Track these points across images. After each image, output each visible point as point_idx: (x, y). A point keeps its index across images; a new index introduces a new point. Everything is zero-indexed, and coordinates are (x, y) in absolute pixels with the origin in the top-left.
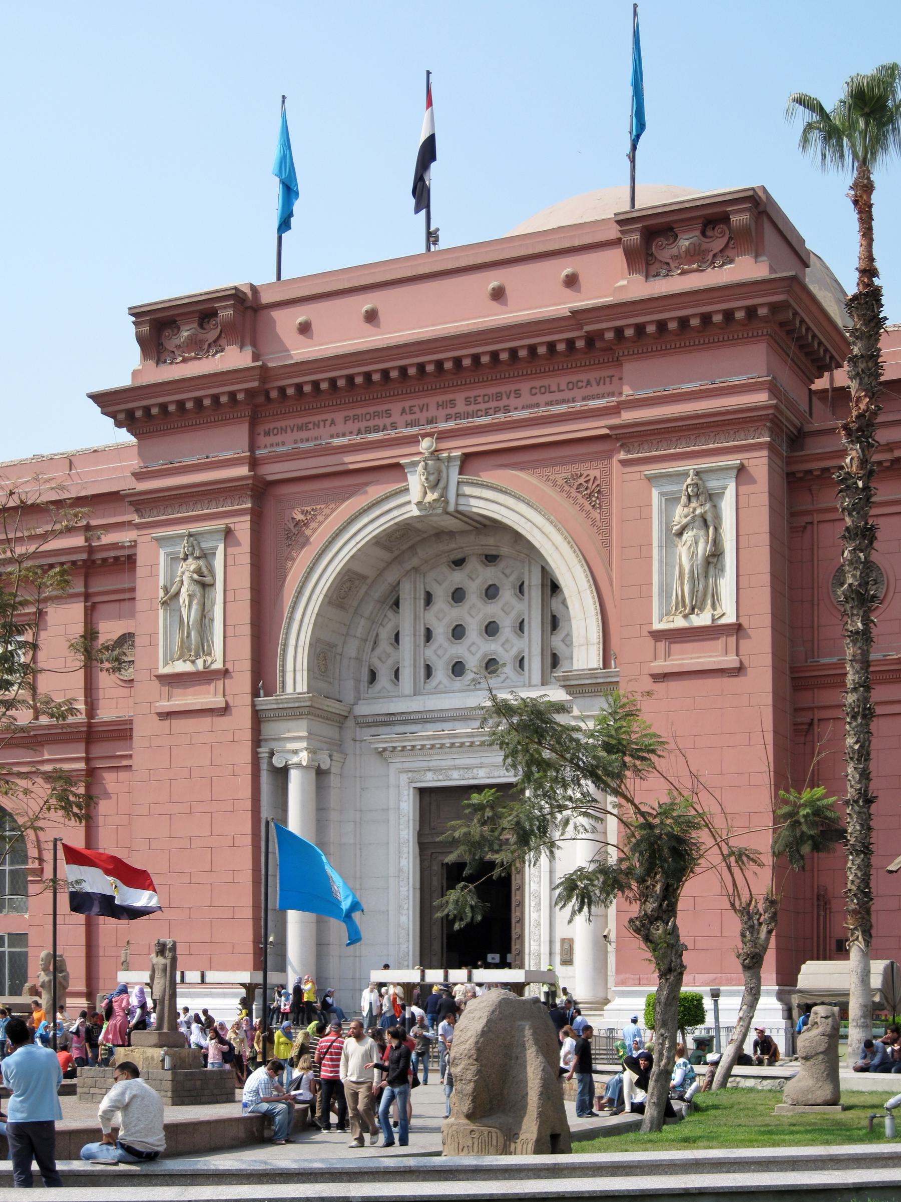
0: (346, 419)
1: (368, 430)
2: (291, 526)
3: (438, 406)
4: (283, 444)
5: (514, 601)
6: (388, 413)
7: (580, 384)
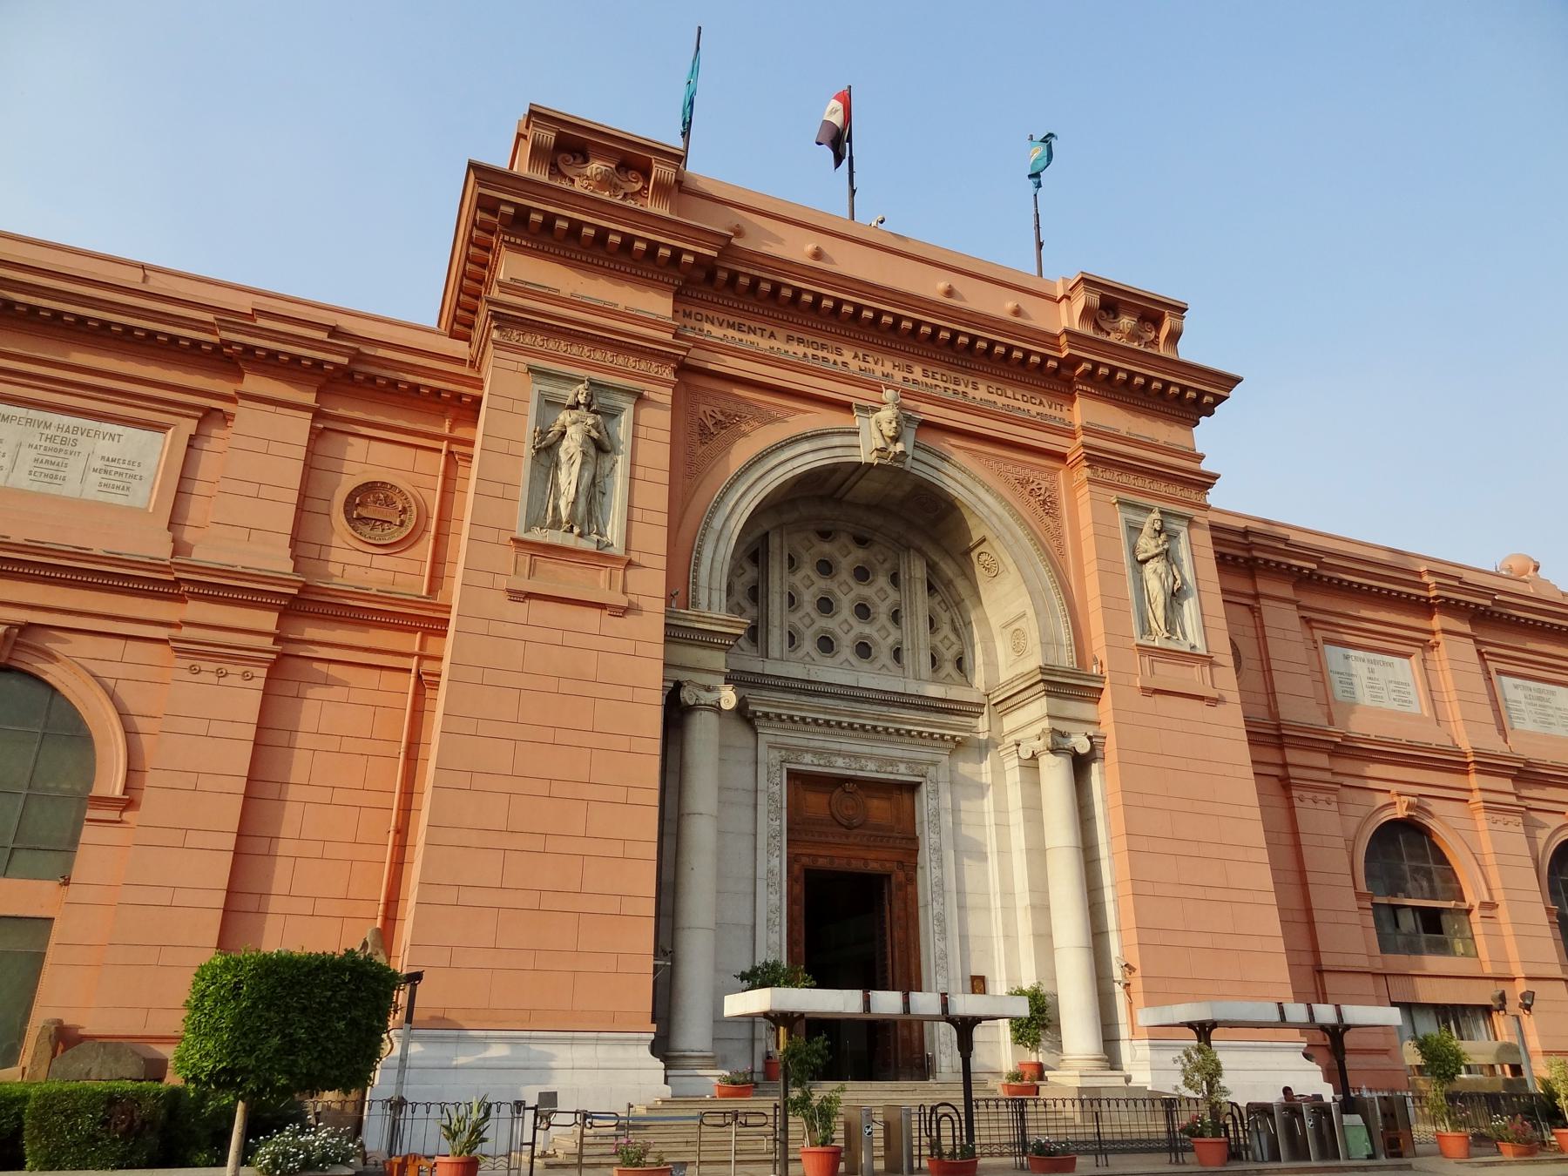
0: (790, 339)
5: (890, 589)
6: (839, 352)
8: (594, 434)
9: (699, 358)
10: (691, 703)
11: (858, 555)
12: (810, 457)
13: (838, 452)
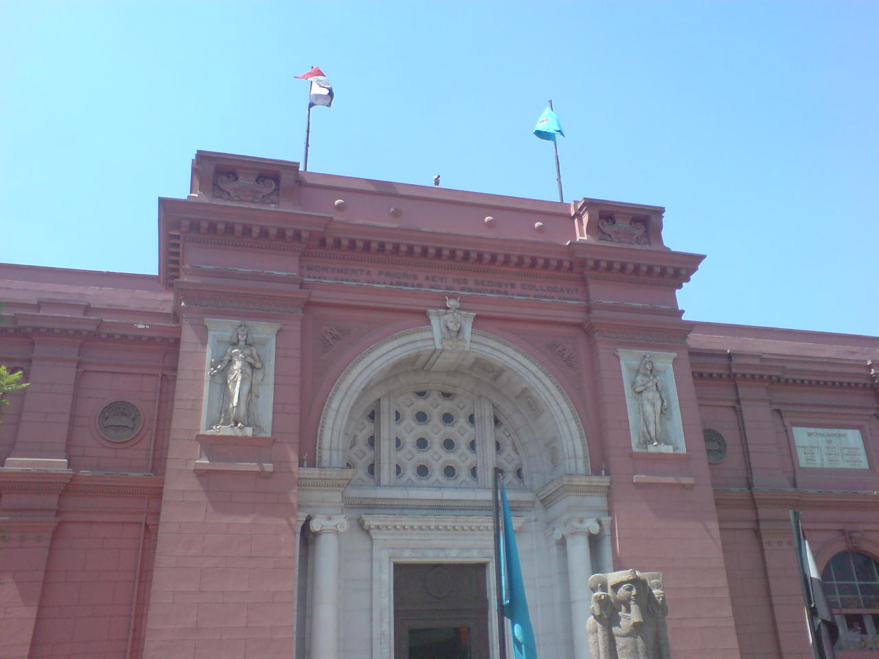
0: (380, 273)
1: (399, 284)
2: (329, 338)
3: (454, 281)
4: (325, 278)
5: (467, 426)
6: (415, 277)
7: (556, 290)
8: (249, 359)
9: (318, 296)
10: (317, 530)
11: (447, 406)
12: (399, 351)
13: (419, 344)
